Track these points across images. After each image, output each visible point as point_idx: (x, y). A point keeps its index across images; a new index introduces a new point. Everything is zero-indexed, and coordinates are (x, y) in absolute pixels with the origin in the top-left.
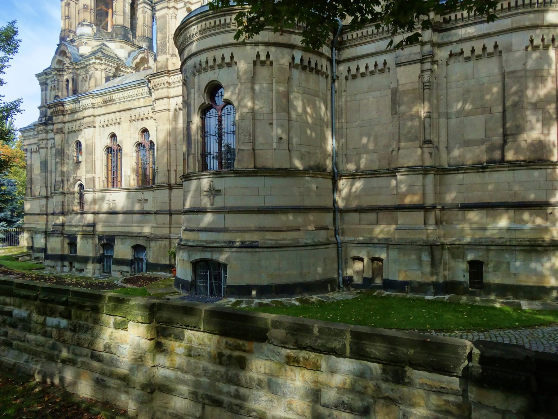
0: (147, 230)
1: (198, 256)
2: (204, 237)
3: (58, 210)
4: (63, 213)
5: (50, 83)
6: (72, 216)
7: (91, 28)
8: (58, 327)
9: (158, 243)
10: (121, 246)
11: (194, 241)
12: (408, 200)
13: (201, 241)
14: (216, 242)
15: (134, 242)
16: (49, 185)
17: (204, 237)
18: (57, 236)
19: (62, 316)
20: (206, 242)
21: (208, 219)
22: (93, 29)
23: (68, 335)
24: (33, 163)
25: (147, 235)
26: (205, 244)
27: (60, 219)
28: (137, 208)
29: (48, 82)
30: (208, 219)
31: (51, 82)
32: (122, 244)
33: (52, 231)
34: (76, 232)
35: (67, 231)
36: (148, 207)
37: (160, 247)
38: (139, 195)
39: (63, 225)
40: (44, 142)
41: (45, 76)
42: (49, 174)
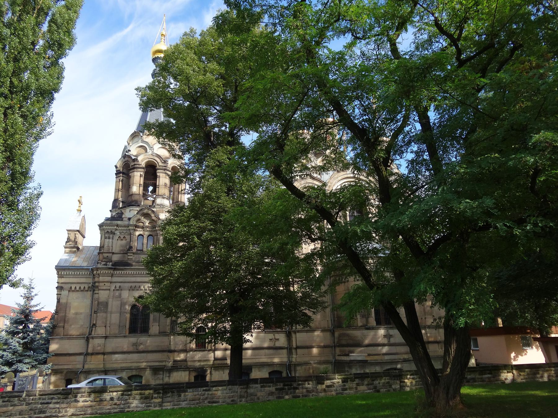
0: (276, 360)
1: (389, 367)
2: (387, 357)
3: (180, 347)
4: (185, 351)
5: (119, 234)
6: (195, 353)
7: (168, 201)
8: (488, 378)
9: (303, 367)
10: (258, 373)
11: (381, 360)
12: (430, 340)
13: (387, 360)
14: (395, 359)
15: (271, 370)
16: (108, 325)
17: (387, 357)
18: (185, 371)
19: (489, 374)
20: (390, 360)
21: (385, 349)
22: (170, 202)
23: (492, 379)
24: (69, 301)
25: (279, 363)
26: (389, 361)
27: (182, 356)
28: (266, 345)
29: (117, 233)
30: (385, 349)
31: (120, 233)
32: (259, 371)
33: (172, 367)
34: (203, 365)
35: (190, 366)
36: (278, 344)
37: (305, 369)
38: (271, 336)
39: (185, 361)
40: (109, 284)
41: (115, 227)
42: (109, 315)
